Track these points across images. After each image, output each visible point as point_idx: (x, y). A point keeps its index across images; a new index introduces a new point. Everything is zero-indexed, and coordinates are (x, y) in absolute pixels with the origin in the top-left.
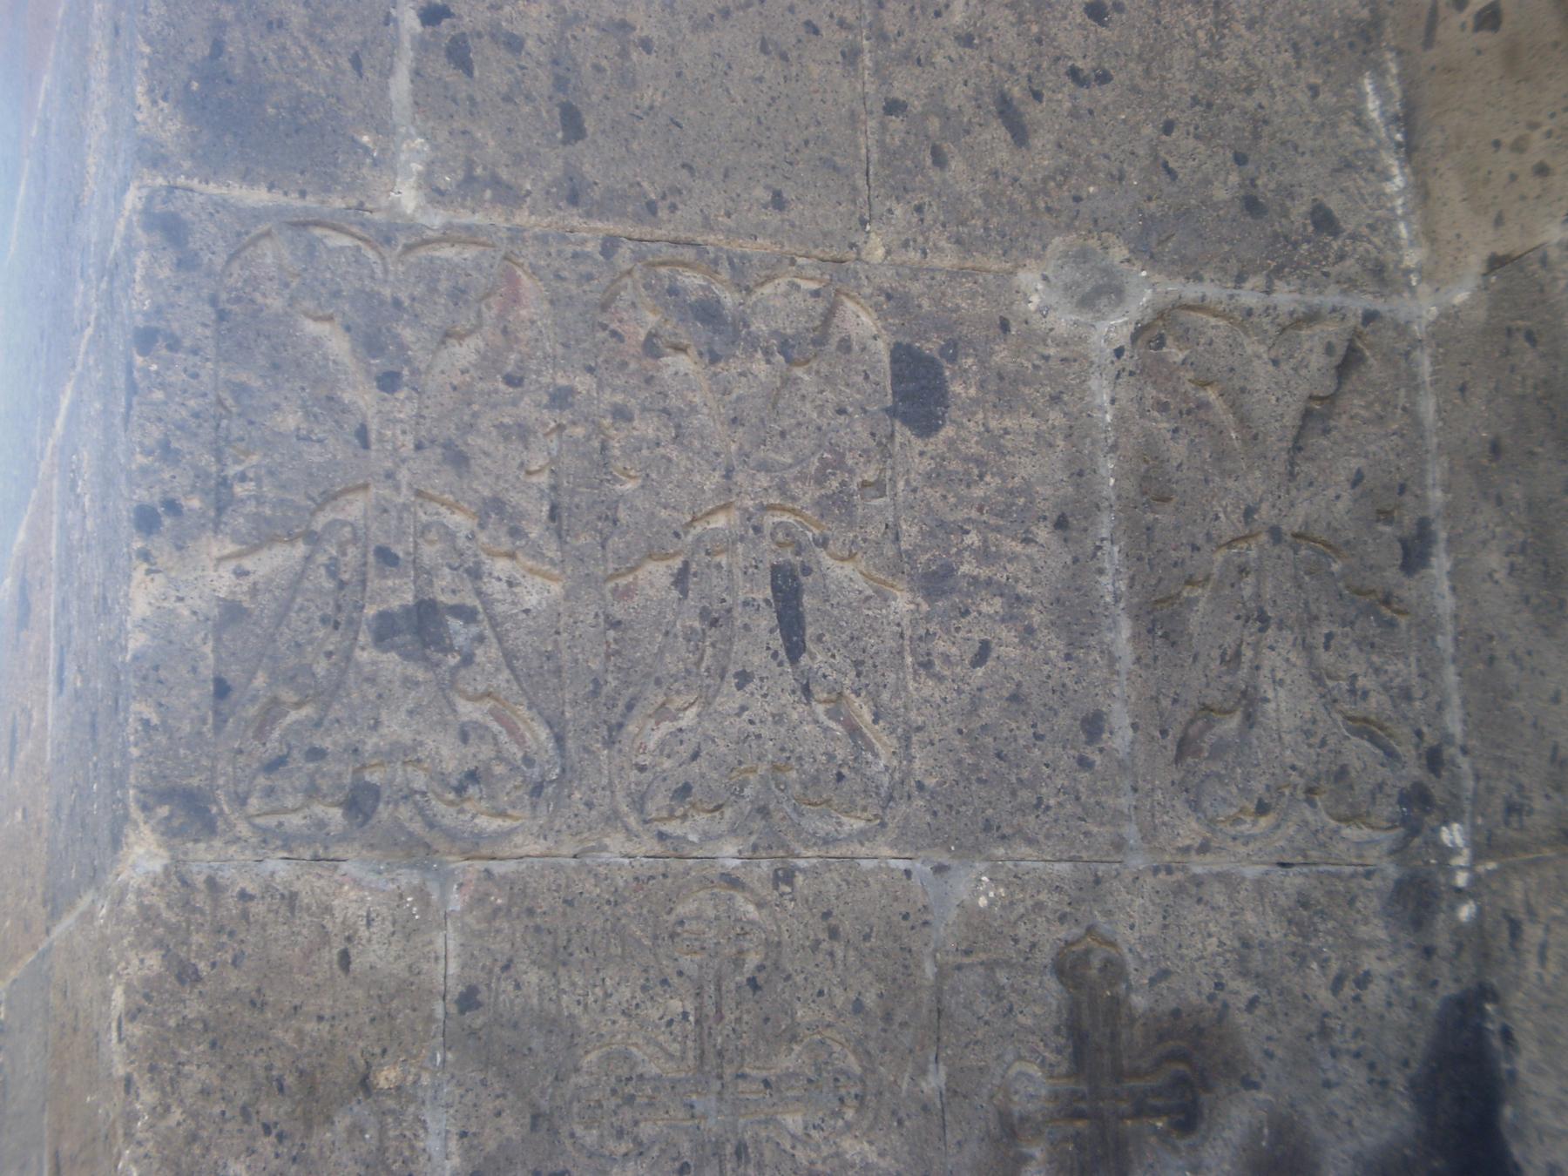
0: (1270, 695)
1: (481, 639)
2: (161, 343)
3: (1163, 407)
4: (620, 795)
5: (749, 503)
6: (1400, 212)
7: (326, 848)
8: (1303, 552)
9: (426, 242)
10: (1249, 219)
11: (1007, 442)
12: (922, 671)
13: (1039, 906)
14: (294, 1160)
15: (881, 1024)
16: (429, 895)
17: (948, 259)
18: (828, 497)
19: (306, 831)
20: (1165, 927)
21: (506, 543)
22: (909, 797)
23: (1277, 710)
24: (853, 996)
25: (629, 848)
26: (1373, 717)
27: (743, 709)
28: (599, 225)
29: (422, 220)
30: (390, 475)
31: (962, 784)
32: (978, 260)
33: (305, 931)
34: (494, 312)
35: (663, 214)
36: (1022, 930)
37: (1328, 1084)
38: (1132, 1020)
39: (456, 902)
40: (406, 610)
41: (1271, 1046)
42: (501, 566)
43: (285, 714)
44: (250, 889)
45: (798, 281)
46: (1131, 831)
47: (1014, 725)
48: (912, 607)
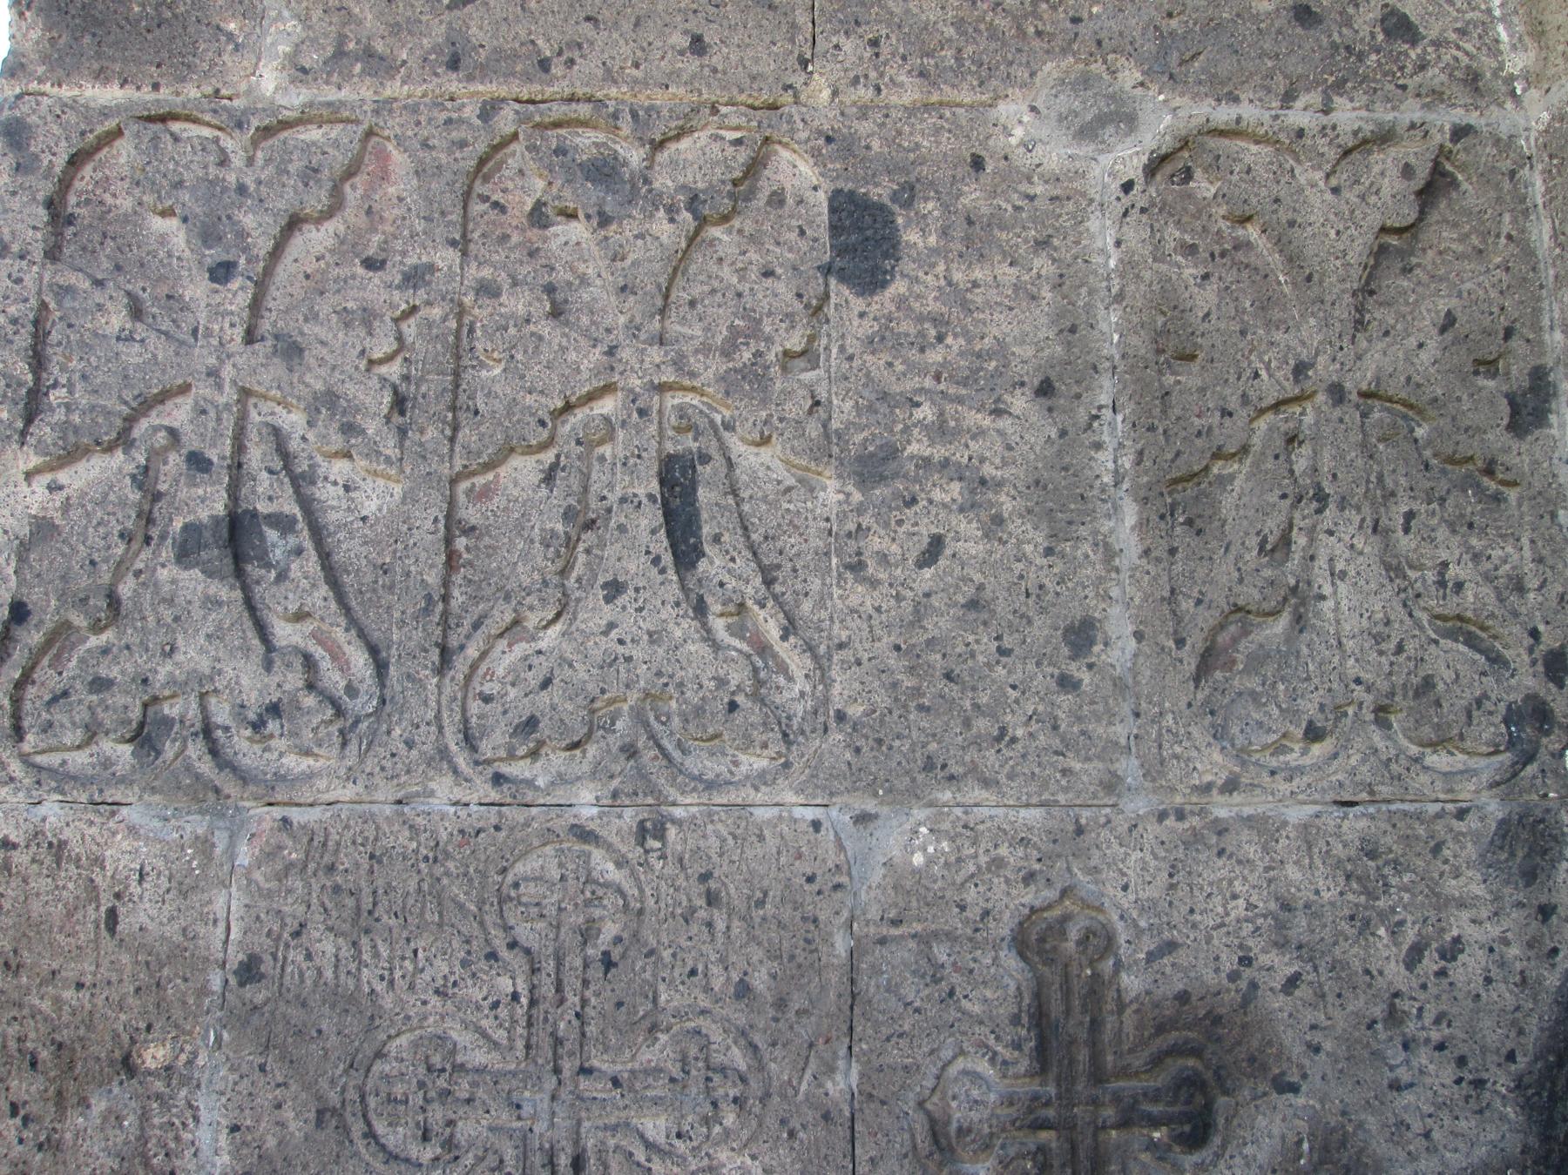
0: (1327, 590)
1: (299, 551)
3: (1190, 250)
5: (635, 382)
6: (1497, 13)
7: (101, 791)
8: (1376, 415)
9: (286, 125)
10: (1299, 30)
11: (977, 297)
12: (849, 575)
13: (998, 864)
14: (40, 1147)
15: (771, 1013)
16: (213, 845)
17: (911, 92)
18: (736, 371)
19: (90, 772)
20: (1172, 887)
21: (337, 441)
22: (826, 730)
23: (1336, 609)
24: (735, 977)
25: (458, 794)
26: (1469, 614)
27: (611, 626)
28: (481, 88)
30: (213, 373)
31: (896, 713)
32: (949, 93)
33: (71, 885)
34: (360, 192)
36: (971, 895)
37: (1396, 1086)
38: (1121, 1007)
39: (245, 856)
40: (216, 520)
41: (1317, 1037)
42: (339, 468)
43: (84, 640)
44: (13, 838)
45: (723, 133)
46: (1129, 768)
47: (971, 638)
48: (841, 497)
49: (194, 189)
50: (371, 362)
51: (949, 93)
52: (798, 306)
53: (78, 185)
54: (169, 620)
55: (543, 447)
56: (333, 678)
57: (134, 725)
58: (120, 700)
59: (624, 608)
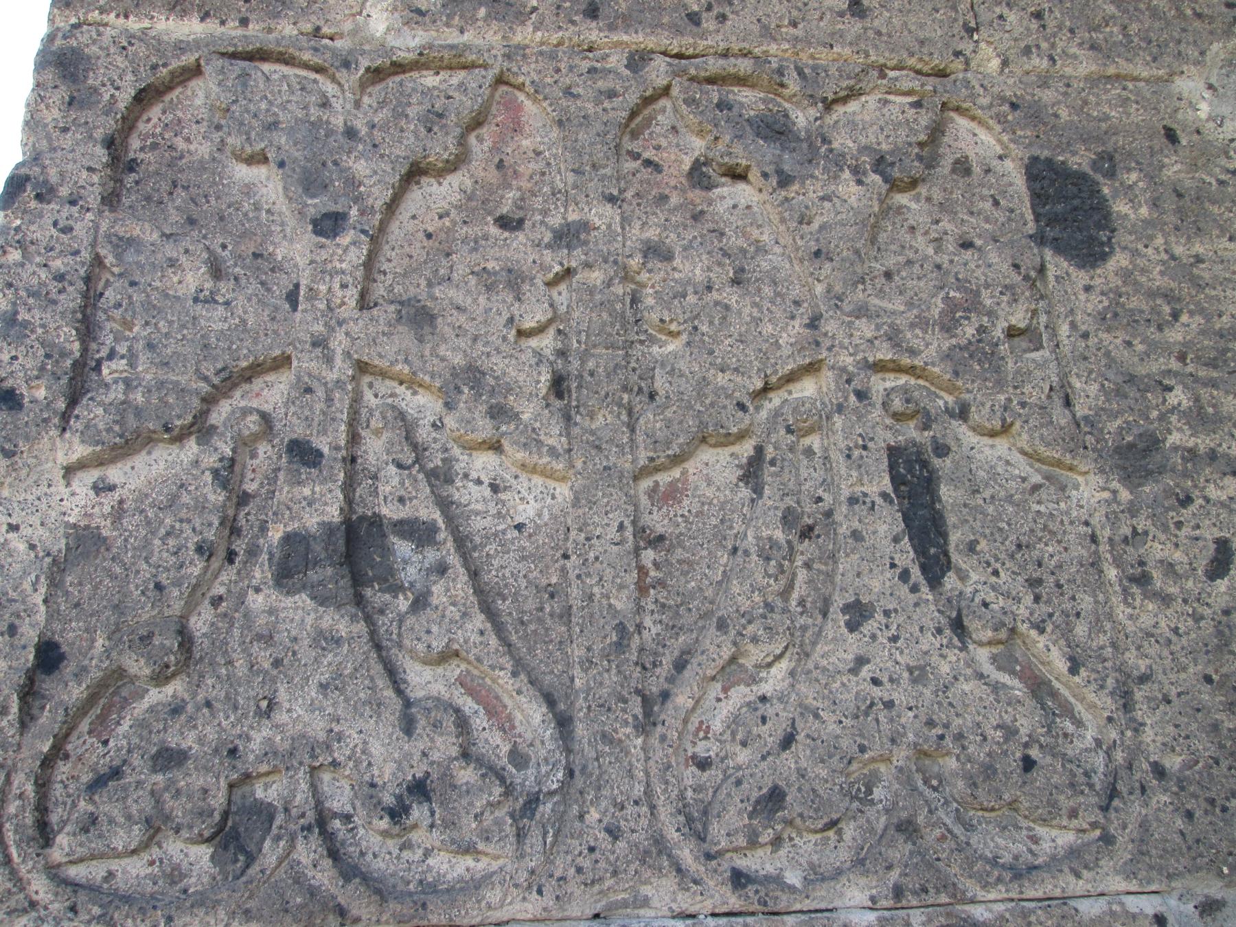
2: (29, 191)
4: (664, 812)
5: (847, 360)
9: (399, 68)
11: (1203, 272)
12: (1135, 589)
17: (1086, 65)
19: (149, 888)
21: (484, 428)
22: (1143, 789)
25: (685, 902)
27: (861, 661)
28: (625, 38)
29: (392, 41)
34: (487, 144)
35: (709, 23)
40: (329, 530)
42: (483, 463)
43: (140, 694)
48: (1106, 495)
49: (291, 131)
50: (521, 333)
51: (1125, 67)
52: (1018, 279)
53: (142, 127)
54: (266, 665)
55: (742, 436)
56: (494, 743)
57: (217, 817)
58: (198, 781)
59: (874, 637)
